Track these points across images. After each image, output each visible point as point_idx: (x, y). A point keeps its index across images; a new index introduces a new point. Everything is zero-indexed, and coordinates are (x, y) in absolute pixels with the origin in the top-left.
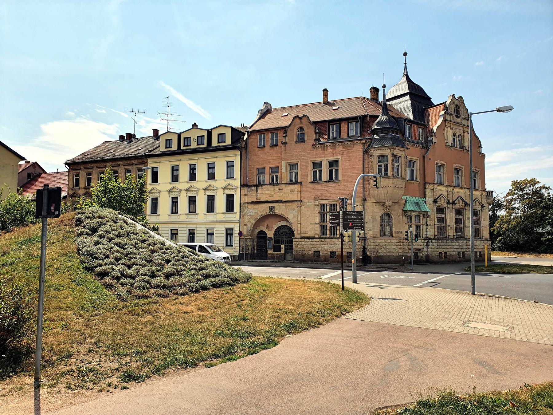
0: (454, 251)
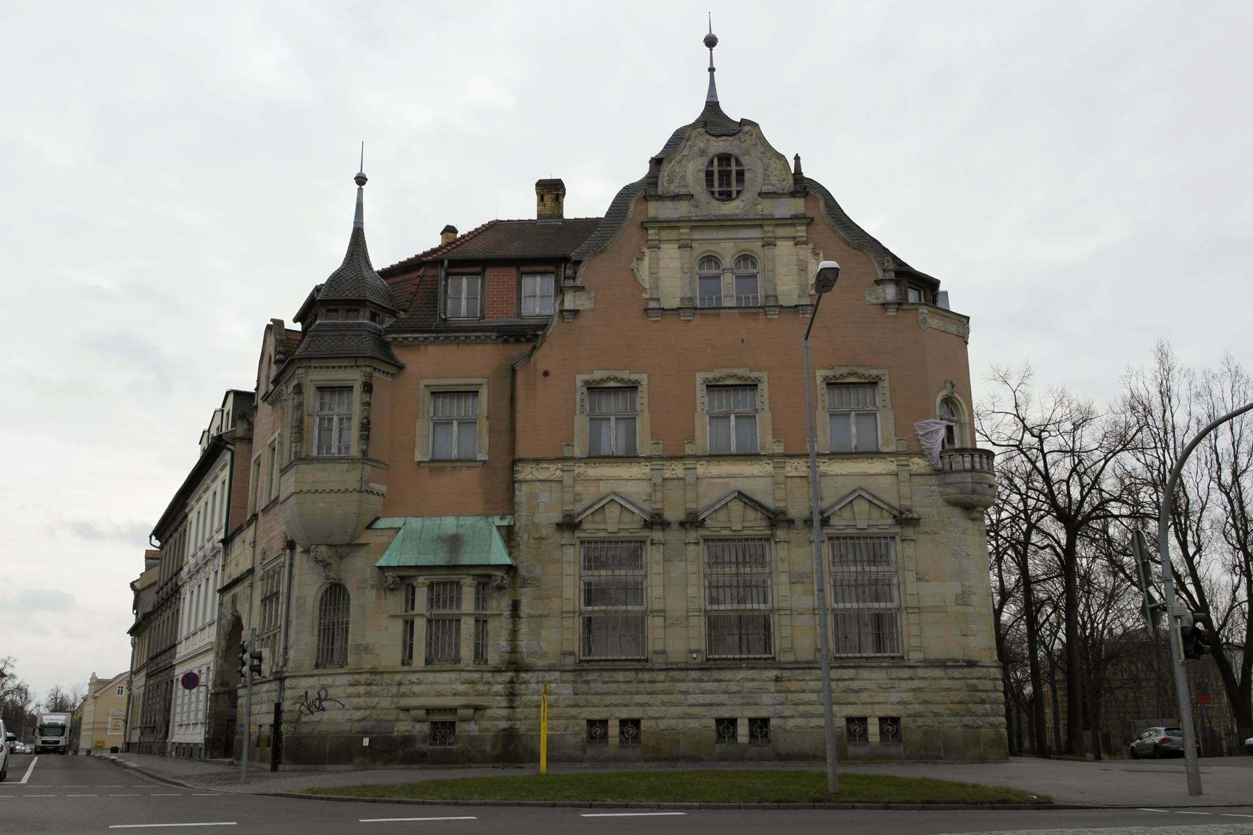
0: (691, 716)
